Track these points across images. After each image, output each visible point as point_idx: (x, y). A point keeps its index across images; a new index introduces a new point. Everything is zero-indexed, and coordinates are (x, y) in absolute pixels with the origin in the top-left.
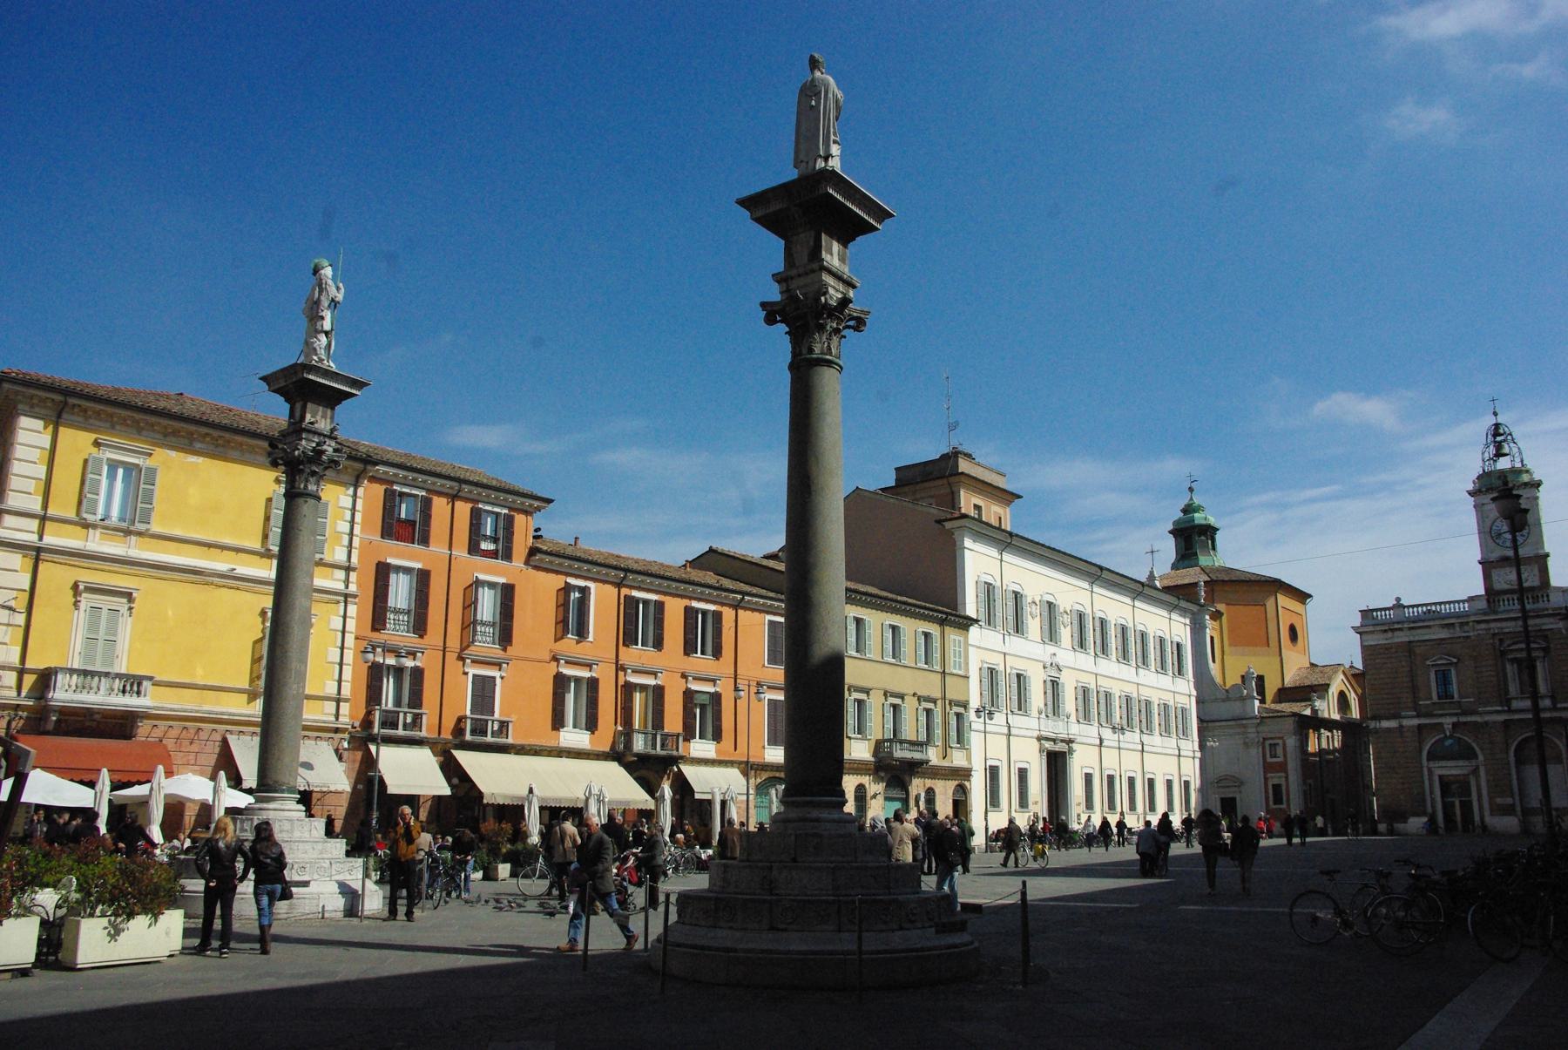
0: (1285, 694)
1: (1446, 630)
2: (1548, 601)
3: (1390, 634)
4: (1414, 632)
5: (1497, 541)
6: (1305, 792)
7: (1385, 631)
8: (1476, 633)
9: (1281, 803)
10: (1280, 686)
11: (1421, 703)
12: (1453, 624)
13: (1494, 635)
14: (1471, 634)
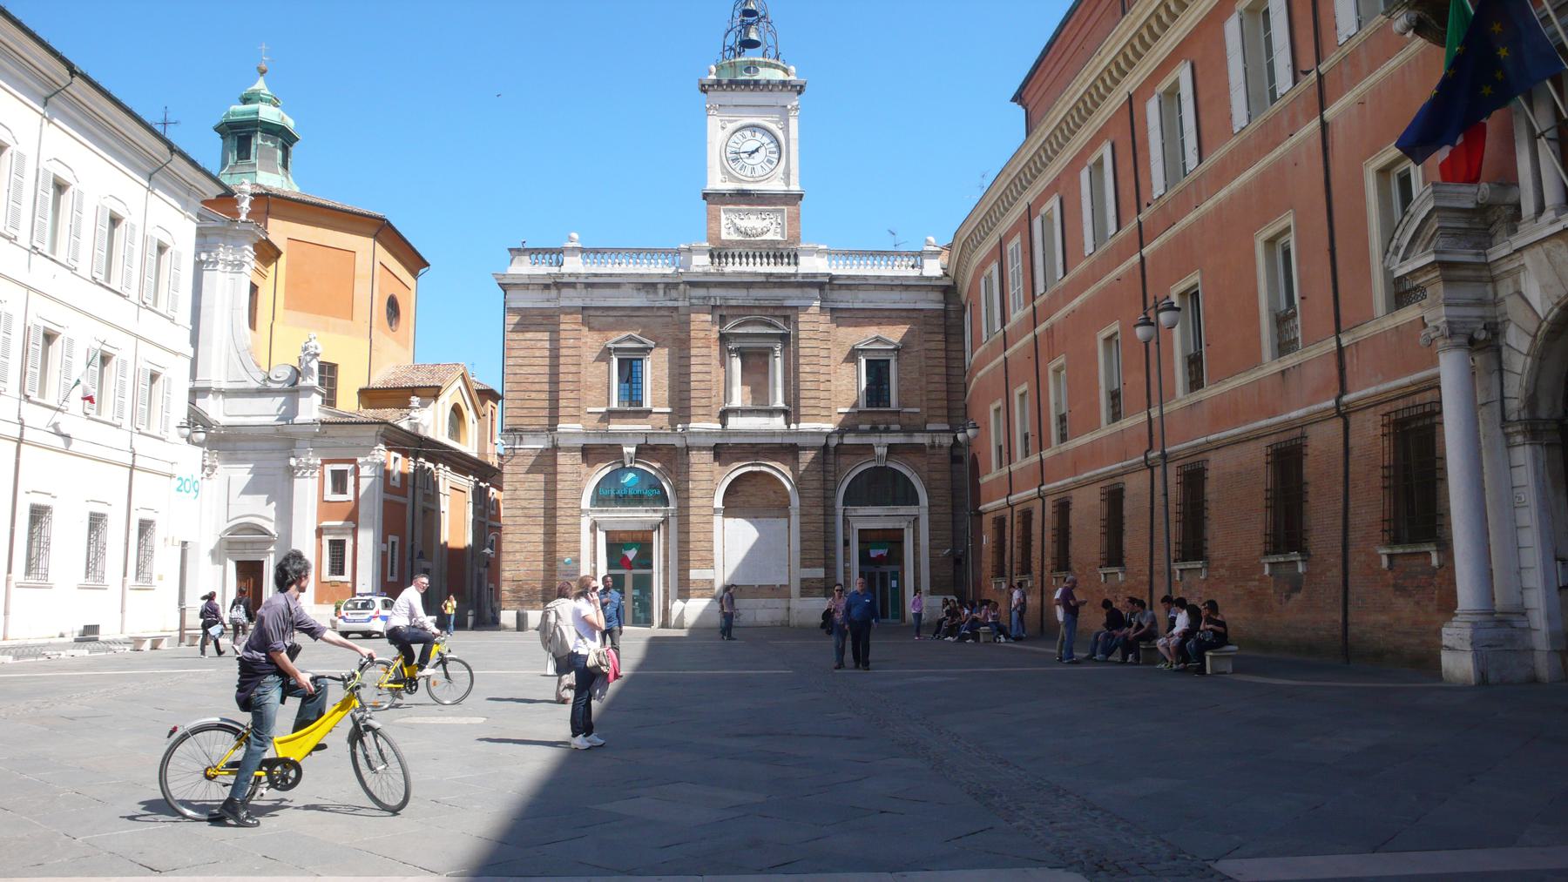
0: (370, 396)
1: (643, 294)
2: (796, 264)
3: (554, 293)
4: (597, 292)
5: (732, 165)
6: (384, 554)
7: (547, 287)
8: (687, 304)
9: (342, 572)
10: (365, 385)
11: (589, 410)
12: (654, 285)
13: (714, 307)
14: (680, 304)
